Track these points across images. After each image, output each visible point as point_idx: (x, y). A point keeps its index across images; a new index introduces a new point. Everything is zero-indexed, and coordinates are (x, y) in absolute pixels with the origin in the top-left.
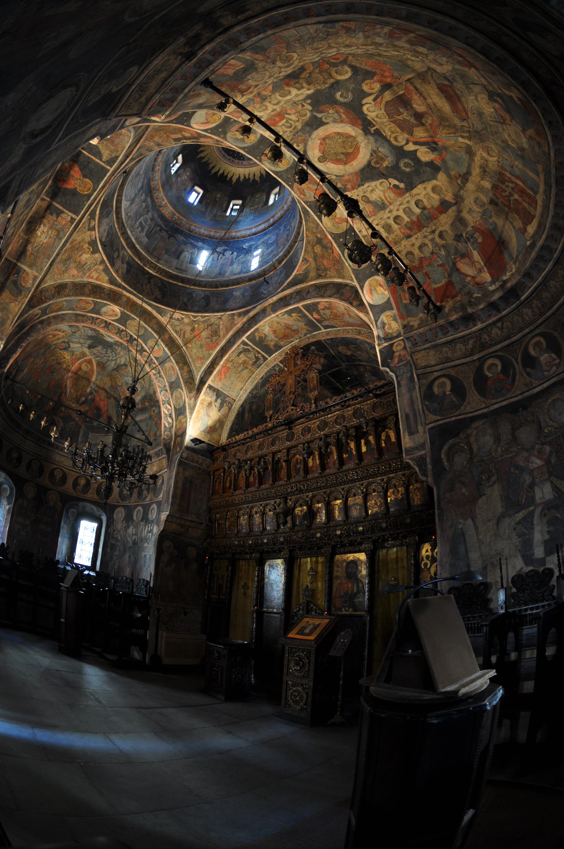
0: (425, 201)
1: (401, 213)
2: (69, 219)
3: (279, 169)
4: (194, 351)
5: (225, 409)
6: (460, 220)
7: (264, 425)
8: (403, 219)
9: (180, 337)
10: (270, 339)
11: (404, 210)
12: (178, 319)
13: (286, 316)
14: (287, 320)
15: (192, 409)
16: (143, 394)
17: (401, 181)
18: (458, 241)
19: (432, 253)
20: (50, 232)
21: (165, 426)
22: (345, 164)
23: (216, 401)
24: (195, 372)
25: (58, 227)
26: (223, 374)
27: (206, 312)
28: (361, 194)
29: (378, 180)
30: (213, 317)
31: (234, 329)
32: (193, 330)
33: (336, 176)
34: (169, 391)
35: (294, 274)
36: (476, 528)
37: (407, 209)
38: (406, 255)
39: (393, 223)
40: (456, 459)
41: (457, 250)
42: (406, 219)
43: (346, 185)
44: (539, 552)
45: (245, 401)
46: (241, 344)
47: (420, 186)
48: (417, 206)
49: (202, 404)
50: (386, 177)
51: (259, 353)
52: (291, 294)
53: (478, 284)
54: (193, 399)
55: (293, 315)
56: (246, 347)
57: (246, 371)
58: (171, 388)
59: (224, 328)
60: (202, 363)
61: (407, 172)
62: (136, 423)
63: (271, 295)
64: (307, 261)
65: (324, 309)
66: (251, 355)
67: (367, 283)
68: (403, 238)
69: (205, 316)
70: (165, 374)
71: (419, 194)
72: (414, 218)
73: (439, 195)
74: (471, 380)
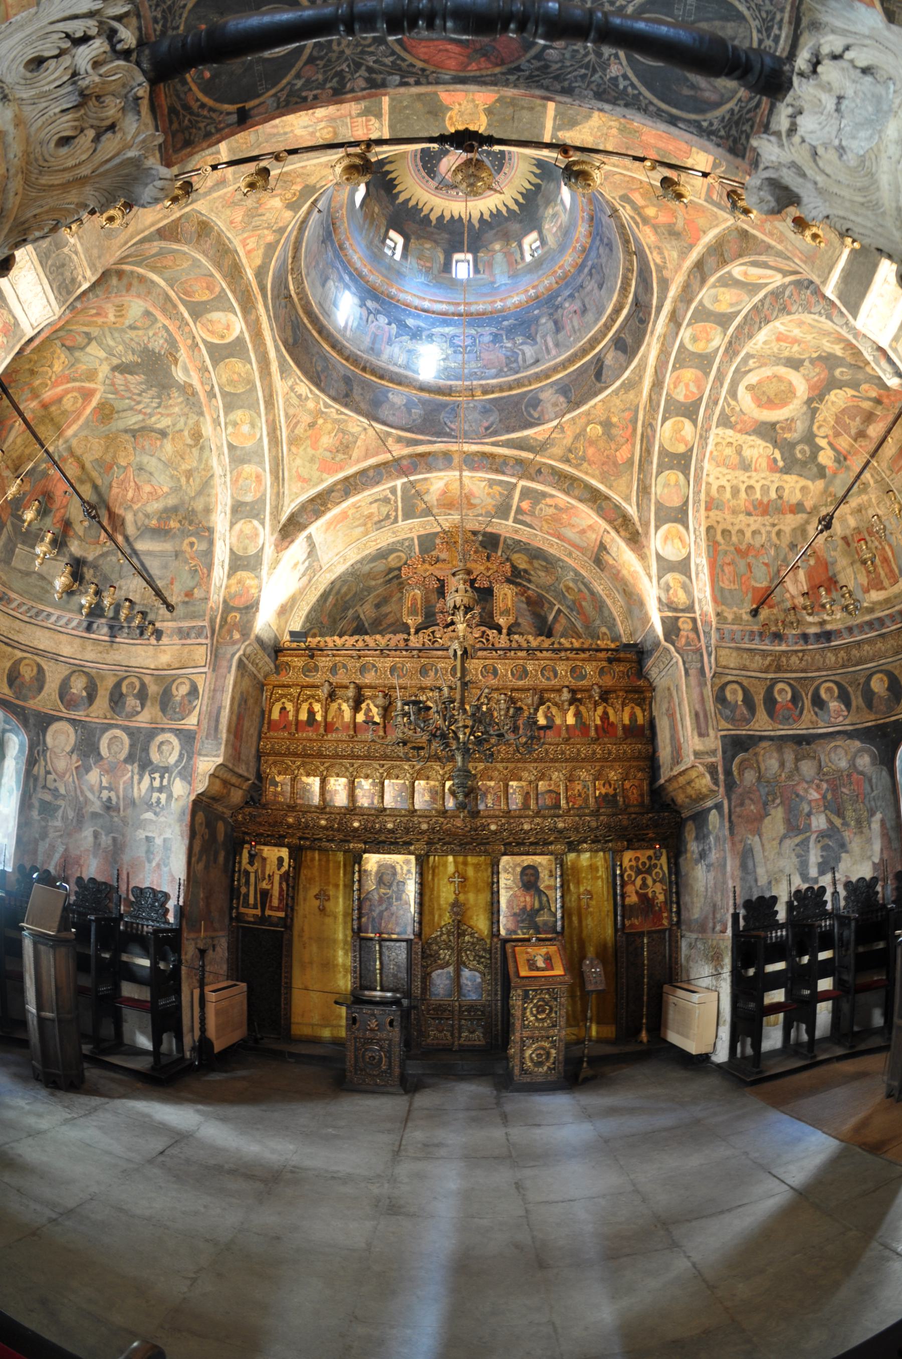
0: (787, 491)
1: (758, 487)
4: (298, 461)
11: (763, 486)
17: (784, 459)
24: (287, 500)
32: (312, 425)
36: (763, 845)
40: (746, 775)
42: (758, 495)
44: (813, 872)
45: (340, 577)
59: (363, 449)
60: (303, 488)
67: (665, 527)
69: (342, 413)
72: (765, 501)
74: (761, 696)
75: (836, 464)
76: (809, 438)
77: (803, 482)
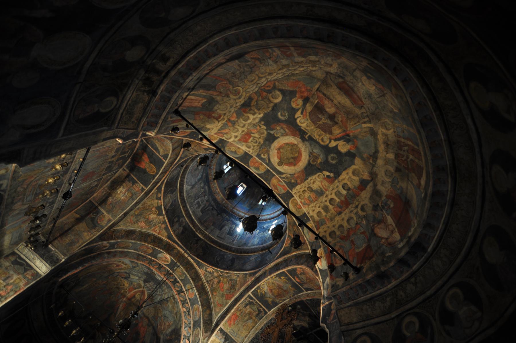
0: (349, 183)
1: (334, 196)
2: (140, 188)
3: (260, 172)
6: (376, 193)
8: (335, 200)
9: (209, 286)
10: (268, 296)
11: (335, 193)
12: (210, 272)
13: (277, 278)
16: (173, 327)
17: (330, 172)
18: (376, 211)
19: (357, 224)
20: (127, 193)
22: (295, 165)
25: (133, 191)
27: (230, 270)
28: (307, 186)
29: (316, 174)
30: (235, 275)
32: (219, 282)
33: (290, 174)
34: (192, 328)
38: (338, 228)
39: (329, 204)
42: (338, 200)
46: (247, 297)
47: (344, 173)
48: (344, 189)
50: (320, 170)
51: (261, 307)
52: (282, 262)
53: (390, 244)
54: (207, 338)
55: (282, 278)
56: (251, 301)
58: (194, 326)
65: (300, 274)
66: (255, 308)
68: (336, 215)
69: (228, 273)
70: (193, 314)
71: (344, 179)
72: (343, 198)
73: (358, 177)
75: (350, 143)
76: (327, 150)
77: (350, 170)
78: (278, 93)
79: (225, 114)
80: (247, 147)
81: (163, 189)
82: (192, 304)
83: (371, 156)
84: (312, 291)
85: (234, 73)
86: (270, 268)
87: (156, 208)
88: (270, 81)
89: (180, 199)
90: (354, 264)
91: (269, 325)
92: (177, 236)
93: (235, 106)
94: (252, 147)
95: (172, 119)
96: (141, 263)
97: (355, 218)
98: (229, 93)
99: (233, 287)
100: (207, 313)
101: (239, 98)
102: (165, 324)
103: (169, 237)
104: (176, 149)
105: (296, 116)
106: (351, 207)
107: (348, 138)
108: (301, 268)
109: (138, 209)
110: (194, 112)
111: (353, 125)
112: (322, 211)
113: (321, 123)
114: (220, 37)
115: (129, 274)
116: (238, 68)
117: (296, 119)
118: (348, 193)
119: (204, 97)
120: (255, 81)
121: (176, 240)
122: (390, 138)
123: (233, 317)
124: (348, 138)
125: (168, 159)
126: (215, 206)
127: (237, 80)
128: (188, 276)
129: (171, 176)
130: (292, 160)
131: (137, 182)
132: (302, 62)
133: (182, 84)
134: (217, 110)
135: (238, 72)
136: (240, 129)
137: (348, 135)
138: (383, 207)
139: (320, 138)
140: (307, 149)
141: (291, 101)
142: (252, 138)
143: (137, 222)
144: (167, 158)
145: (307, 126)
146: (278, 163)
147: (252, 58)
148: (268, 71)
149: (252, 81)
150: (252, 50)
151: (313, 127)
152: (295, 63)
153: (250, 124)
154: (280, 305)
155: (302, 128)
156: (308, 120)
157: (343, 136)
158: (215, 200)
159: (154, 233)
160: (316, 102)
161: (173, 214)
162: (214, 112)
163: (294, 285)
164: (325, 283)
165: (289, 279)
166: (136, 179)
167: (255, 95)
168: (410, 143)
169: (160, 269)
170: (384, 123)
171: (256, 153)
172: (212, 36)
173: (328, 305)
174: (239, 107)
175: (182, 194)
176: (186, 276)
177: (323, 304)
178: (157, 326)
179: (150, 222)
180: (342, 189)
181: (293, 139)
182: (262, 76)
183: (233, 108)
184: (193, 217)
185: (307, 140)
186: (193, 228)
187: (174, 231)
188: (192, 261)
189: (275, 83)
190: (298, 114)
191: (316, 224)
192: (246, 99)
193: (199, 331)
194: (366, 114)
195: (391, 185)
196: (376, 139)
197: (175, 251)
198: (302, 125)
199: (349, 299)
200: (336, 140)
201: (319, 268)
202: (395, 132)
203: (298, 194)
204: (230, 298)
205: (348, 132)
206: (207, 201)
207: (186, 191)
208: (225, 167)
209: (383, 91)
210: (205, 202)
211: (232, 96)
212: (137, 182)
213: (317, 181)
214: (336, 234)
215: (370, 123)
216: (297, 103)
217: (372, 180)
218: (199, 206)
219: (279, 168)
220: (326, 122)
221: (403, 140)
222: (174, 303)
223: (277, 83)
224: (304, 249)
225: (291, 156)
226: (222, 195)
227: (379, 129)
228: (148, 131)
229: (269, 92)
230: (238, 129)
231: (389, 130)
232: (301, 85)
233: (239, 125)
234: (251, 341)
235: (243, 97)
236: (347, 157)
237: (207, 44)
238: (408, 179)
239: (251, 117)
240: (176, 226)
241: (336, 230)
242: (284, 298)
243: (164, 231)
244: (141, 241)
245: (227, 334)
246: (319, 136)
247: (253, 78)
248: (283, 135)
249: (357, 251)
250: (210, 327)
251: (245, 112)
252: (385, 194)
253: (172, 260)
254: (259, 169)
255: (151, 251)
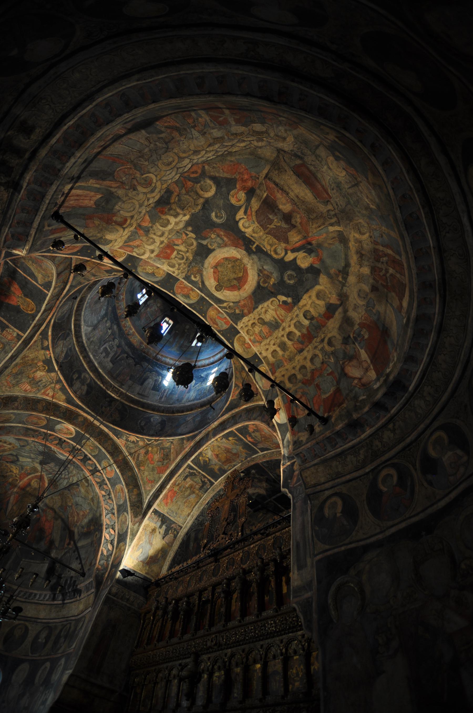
0: (312, 310)
1: (292, 329)
2: (15, 335)
3: (191, 302)
5: (170, 536)
6: (347, 321)
7: (198, 556)
8: (295, 334)
9: (133, 459)
11: (295, 325)
12: (133, 442)
13: (224, 440)
14: (226, 444)
15: (134, 535)
16: (90, 516)
17: (287, 296)
18: (346, 344)
19: (322, 363)
21: (102, 554)
22: (239, 289)
23: (161, 527)
24: (144, 495)
26: (169, 498)
27: (160, 436)
28: (257, 317)
29: (268, 299)
30: (167, 441)
31: (183, 453)
32: (147, 453)
33: (233, 302)
34: (116, 515)
35: (230, 400)
37: (297, 323)
38: (300, 370)
39: (286, 340)
41: (345, 353)
43: (243, 311)
45: (191, 529)
46: (187, 467)
47: (305, 296)
48: (306, 318)
49: (145, 529)
50: (274, 295)
52: (228, 419)
53: (364, 385)
54: (137, 524)
55: (230, 438)
56: (192, 471)
57: (194, 495)
58: (118, 511)
60: (152, 486)
61: (288, 283)
62: (77, 548)
63: (214, 420)
64: (239, 387)
65: (253, 432)
66: (198, 479)
68: (297, 354)
69: (158, 440)
70: (115, 496)
71: (305, 305)
72: (305, 331)
73: (324, 300)
75: (313, 255)
76: (282, 265)
77: (313, 293)
78: (209, 182)
79: (132, 217)
80: (170, 266)
81: (50, 333)
82: (113, 485)
83: (340, 271)
84: (269, 451)
85: (140, 152)
86: (214, 428)
87: (44, 362)
88: (197, 164)
89: (78, 346)
90: (320, 414)
91: (217, 498)
92: (79, 398)
93: (146, 203)
94: (177, 266)
95: (50, 228)
96: (32, 439)
97: (320, 356)
98: (136, 184)
99: (166, 457)
100: (135, 493)
101: (152, 191)
102: (78, 514)
103: (69, 400)
104: (63, 274)
105: (238, 218)
106: (316, 341)
107: (309, 247)
108: (253, 425)
109: (16, 365)
110: (84, 215)
111: (316, 228)
112: (278, 349)
113: (272, 226)
114: (114, 92)
115: (16, 456)
116: (147, 143)
117: (237, 222)
118: (310, 323)
119: (98, 190)
120: (174, 164)
121: (80, 404)
122: (365, 246)
123: (170, 494)
124: (309, 247)
125: (52, 289)
126: (130, 353)
127: (147, 163)
128: (103, 450)
129: (60, 314)
130: (235, 282)
131: (8, 327)
132: (242, 134)
133: (59, 171)
134: (119, 211)
135: (146, 150)
136: (158, 240)
137: (310, 243)
138: (355, 338)
139: (272, 249)
140: (255, 265)
141: (228, 194)
142: (175, 253)
143: (17, 384)
144: (50, 287)
145: (254, 231)
146: (215, 288)
147: (166, 127)
148: (192, 147)
149: (170, 163)
150: (166, 114)
151: (261, 234)
152: (233, 134)
153: (171, 231)
154: (230, 472)
155: (247, 235)
156: (254, 223)
157: (304, 245)
158: (130, 345)
159: (45, 397)
160: (265, 195)
161: (70, 368)
162: (114, 215)
163: (246, 446)
164: (285, 440)
165: (241, 440)
166: (5, 322)
167: (175, 186)
168: (390, 252)
169: (61, 445)
170: (357, 225)
171: (184, 274)
172: (100, 90)
173: (289, 465)
174: (152, 205)
175: (80, 340)
176: (100, 450)
177: (283, 465)
178: (68, 518)
179: (37, 383)
180: (303, 318)
181: (235, 252)
182: (184, 155)
183: (144, 207)
184: (100, 371)
185: (254, 253)
186: (102, 385)
187: (75, 392)
188: (106, 430)
189: (204, 167)
190: (240, 214)
191: (271, 367)
192: (162, 192)
193: (126, 517)
194: (333, 213)
195: (366, 311)
196: (347, 247)
197: (80, 419)
198: (246, 230)
199: (316, 456)
200: (293, 251)
201: (277, 422)
202: (371, 237)
203: (246, 329)
204: (163, 472)
205: (309, 239)
206: (118, 347)
207: (86, 334)
208: (139, 296)
209: (356, 179)
210: (115, 348)
211: (140, 188)
212: (8, 327)
213: (270, 309)
214: (296, 378)
215: (340, 226)
216: (238, 197)
217: (341, 305)
218: (107, 354)
219: (218, 295)
220: (279, 224)
221: (381, 248)
222: (88, 486)
223: (206, 167)
224: (257, 401)
225: (233, 276)
226: (138, 337)
227: (350, 233)
228: (14, 248)
229: (196, 180)
230: (154, 239)
231: (363, 234)
232: (242, 170)
233: (155, 234)
234: (196, 519)
235: (157, 190)
236: (309, 275)
237: (94, 103)
238: (387, 301)
239: (173, 220)
240: (77, 385)
241: (296, 373)
242: (234, 463)
243: (60, 393)
244: (27, 410)
245: (164, 515)
246: (271, 245)
247: (171, 159)
248: (220, 246)
249: (324, 396)
250: (140, 510)
251: (163, 213)
252: (358, 321)
253: (76, 431)
254: (189, 297)
255: (45, 423)
